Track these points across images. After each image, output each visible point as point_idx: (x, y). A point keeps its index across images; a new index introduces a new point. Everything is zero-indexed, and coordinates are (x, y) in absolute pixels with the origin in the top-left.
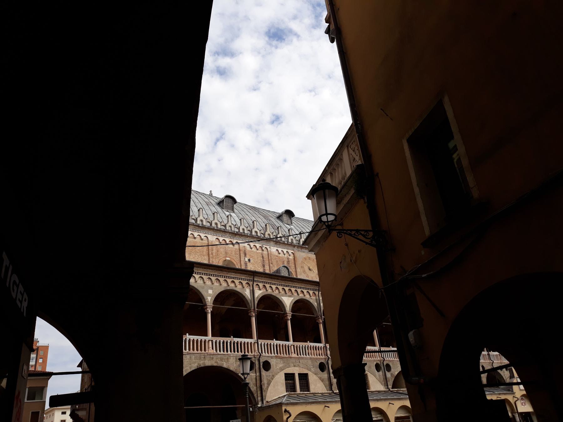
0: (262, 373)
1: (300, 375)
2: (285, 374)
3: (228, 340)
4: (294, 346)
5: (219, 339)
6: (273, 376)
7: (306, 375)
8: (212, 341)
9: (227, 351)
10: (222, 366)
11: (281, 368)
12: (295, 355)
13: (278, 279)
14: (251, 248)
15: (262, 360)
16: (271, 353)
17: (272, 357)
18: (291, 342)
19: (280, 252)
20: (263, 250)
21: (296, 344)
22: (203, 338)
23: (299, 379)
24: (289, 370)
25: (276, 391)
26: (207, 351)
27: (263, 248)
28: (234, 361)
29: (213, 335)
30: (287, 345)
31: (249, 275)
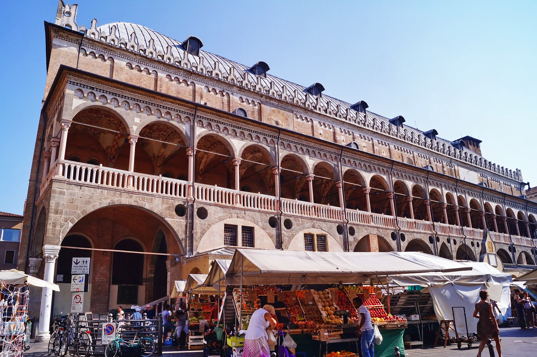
0: (194, 220)
1: (243, 227)
2: (225, 225)
3: (156, 178)
4: (240, 195)
5: (142, 176)
8: (133, 177)
9: (152, 191)
10: (144, 206)
12: (241, 206)
16: (210, 200)
18: (237, 191)
20: (223, 96)
21: (243, 193)
23: (243, 232)
24: (231, 221)
27: (224, 94)
28: (160, 202)
29: (136, 170)
30: (231, 193)
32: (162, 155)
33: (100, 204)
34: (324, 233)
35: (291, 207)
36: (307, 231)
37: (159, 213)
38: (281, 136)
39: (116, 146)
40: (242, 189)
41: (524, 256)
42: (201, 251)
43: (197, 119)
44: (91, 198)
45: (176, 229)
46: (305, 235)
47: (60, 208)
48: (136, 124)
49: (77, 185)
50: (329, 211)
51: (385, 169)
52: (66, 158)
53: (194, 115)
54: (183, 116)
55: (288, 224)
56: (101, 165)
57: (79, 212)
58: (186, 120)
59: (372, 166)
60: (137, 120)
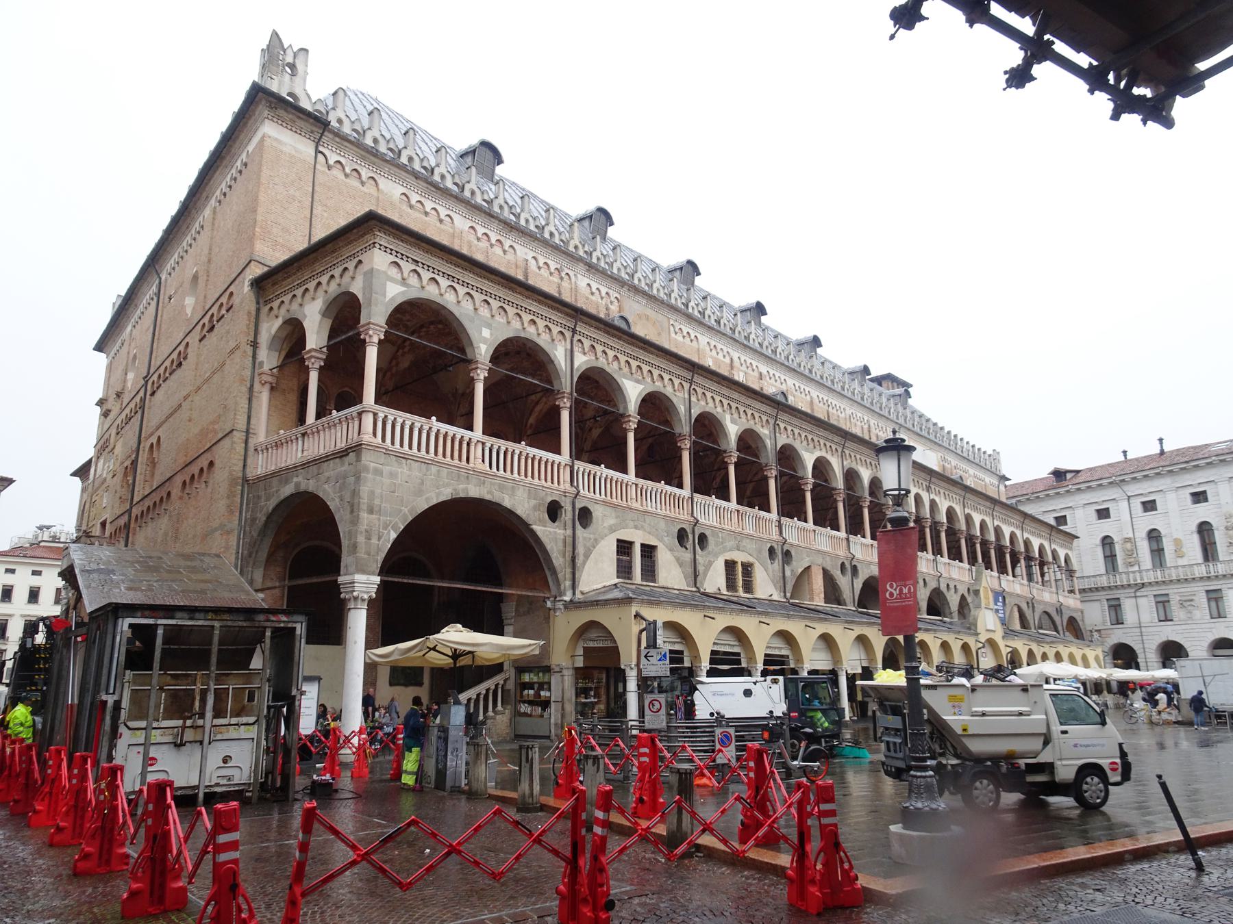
1: (642, 545)
2: (618, 541)
6: (596, 540)
7: (653, 548)
11: (611, 526)
13: (620, 339)
14: (539, 268)
15: (579, 505)
17: (596, 502)
18: (631, 476)
19: (594, 290)
20: (562, 278)
21: (641, 482)
22: (460, 432)
24: (626, 535)
25: (598, 573)
26: (471, 465)
27: (563, 274)
28: (525, 495)
31: (567, 314)
32: (521, 401)
33: (438, 495)
34: (751, 560)
35: (717, 514)
36: (730, 556)
37: (524, 516)
38: (697, 379)
39: (394, 370)
40: (637, 476)
41: (1016, 609)
42: (586, 589)
43: (577, 337)
44: (422, 483)
45: (548, 548)
46: (727, 562)
47: (377, 502)
48: (485, 341)
49: (418, 460)
50: (757, 518)
51: (834, 447)
52: (378, 400)
53: (574, 331)
54: (556, 330)
55: (703, 539)
56: (434, 418)
57: (405, 510)
58: (561, 337)
59: (816, 439)
60: (486, 333)
